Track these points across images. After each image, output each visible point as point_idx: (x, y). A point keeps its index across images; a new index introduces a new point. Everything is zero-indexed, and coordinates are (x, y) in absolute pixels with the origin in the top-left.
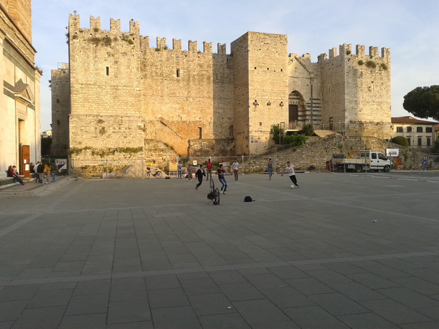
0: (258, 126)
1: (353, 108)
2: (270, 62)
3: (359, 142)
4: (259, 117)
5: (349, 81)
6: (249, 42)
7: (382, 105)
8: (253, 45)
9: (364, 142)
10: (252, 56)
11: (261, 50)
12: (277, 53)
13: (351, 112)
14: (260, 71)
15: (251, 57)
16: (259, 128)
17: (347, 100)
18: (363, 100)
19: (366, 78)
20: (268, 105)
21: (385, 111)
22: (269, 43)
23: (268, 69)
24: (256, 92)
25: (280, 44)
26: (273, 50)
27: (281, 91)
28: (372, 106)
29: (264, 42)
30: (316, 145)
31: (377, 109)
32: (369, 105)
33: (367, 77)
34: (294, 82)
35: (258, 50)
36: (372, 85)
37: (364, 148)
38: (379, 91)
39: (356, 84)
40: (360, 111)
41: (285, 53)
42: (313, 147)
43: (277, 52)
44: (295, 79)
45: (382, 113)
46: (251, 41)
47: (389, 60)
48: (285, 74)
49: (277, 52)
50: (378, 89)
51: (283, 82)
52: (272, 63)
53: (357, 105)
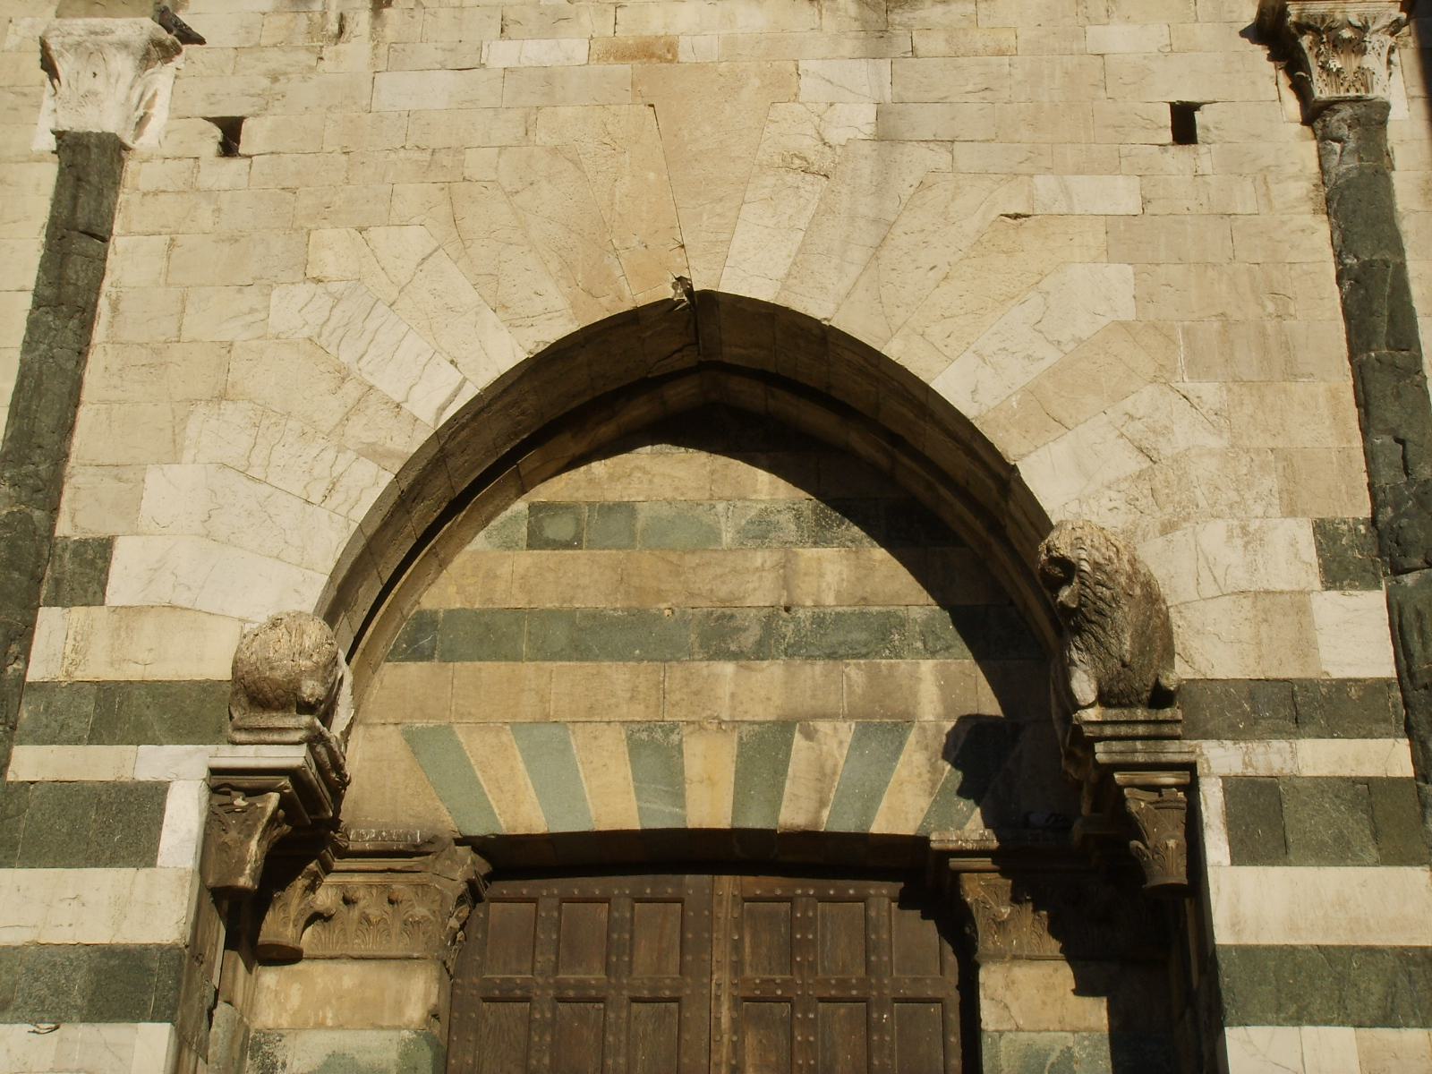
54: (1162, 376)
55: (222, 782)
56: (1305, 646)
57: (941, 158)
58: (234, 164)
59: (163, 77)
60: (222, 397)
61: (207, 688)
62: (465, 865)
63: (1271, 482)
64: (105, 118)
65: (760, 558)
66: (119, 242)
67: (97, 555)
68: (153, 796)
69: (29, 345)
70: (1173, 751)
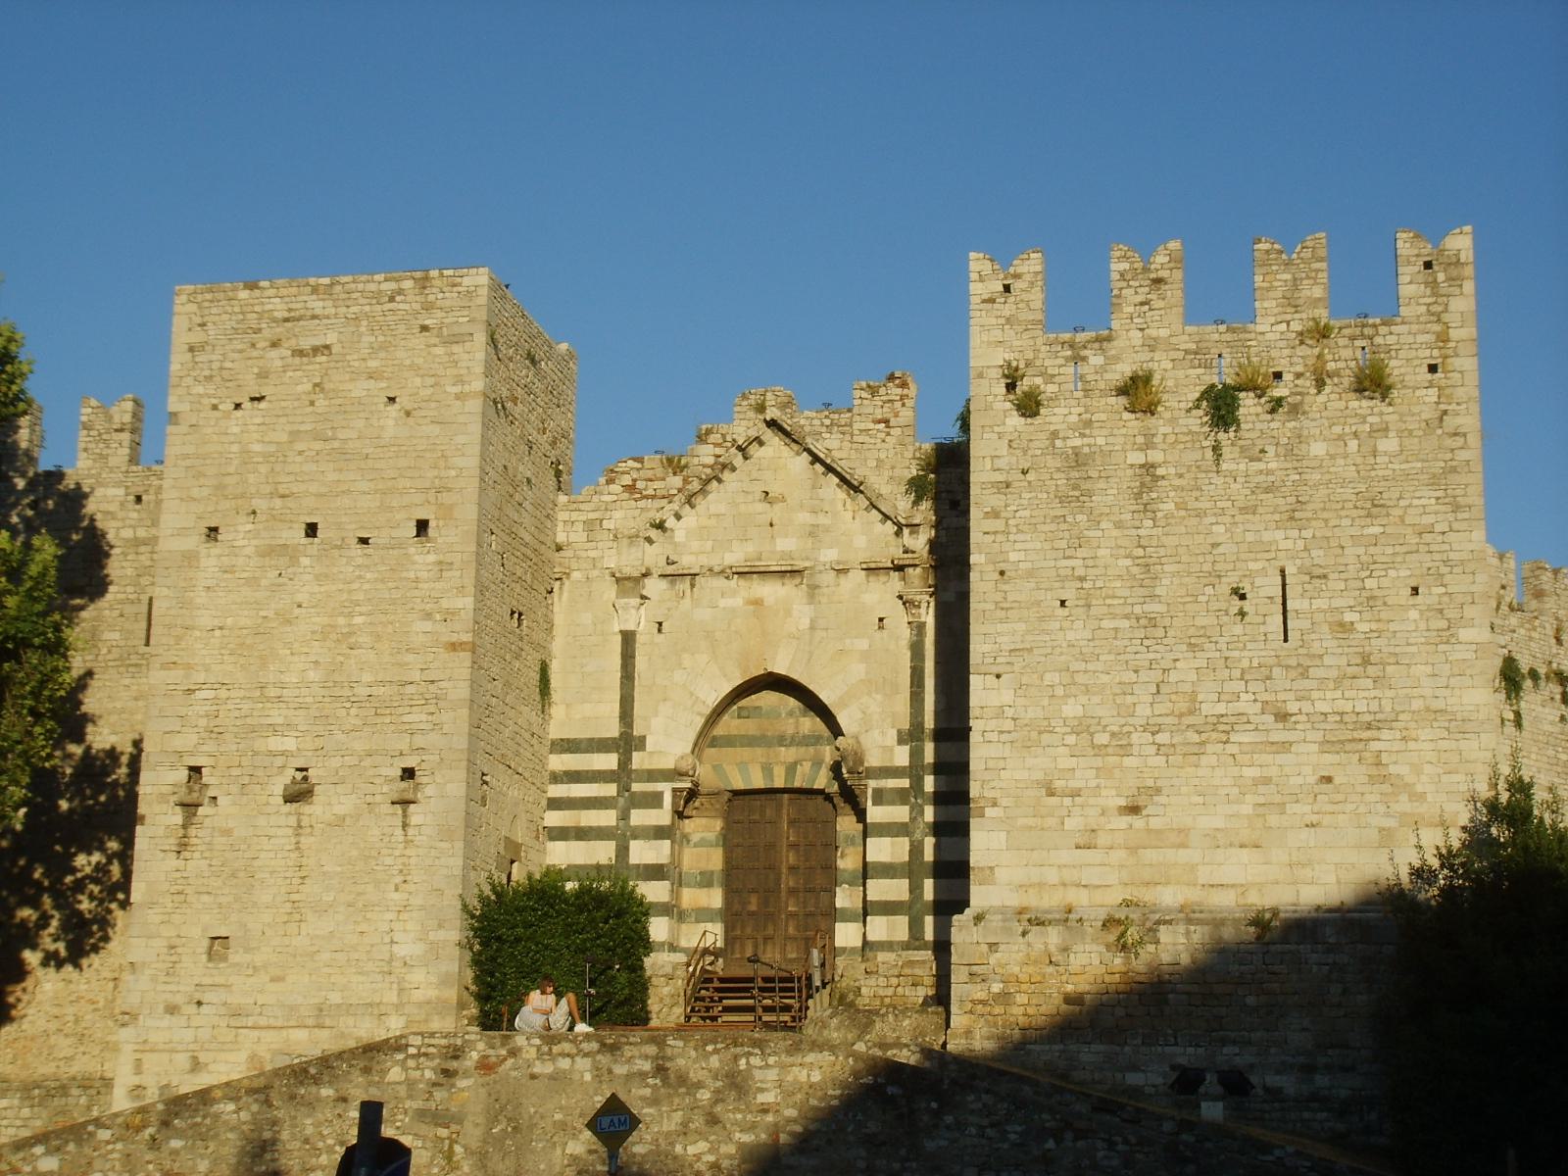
0: (194, 966)
1: (1059, 784)
2: (333, 476)
3: (647, 1092)
4: (205, 898)
5: (1013, 557)
6: (178, 361)
7: (1386, 741)
8: (209, 378)
9: (699, 1085)
10: (190, 450)
11: (263, 405)
12: (393, 409)
13: (1031, 822)
14: (249, 551)
15: (186, 456)
16: (207, 981)
17: (992, 724)
18: (1159, 709)
19: (1200, 514)
20: (291, 798)
21: (1422, 796)
22: (327, 347)
23: (312, 530)
24: (202, 709)
25: (419, 341)
26: (359, 389)
27: (410, 689)
28: (1267, 758)
29: (293, 342)
30: (217, 1116)
31: (1328, 780)
32: (1232, 749)
33: (1205, 505)
34: (757, 603)
35: (238, 406)
36: (1264, 572)
37: (691, 1150)
38: (1349, 617)
39: (1082, 579)
40: (1134, 810)
41: (458, 397)
42: (180, 1134)
43: (392, 400)
44: (770, 591)
45: (1391, 823)
46: (191, 349)
47: (1453, 334)
48: (448, 558)
49: (392, 400)
50: (1337, 603)
51: (428, 616)
52: (345, 487)
53: (1098, 762)
54: (869, 694)
55: (674, 790)
56: (891, 759)
57: (824, 634)
58: (662, 636)
59: (643, 609)
60: (665, 700)
61: (669, 770)
62: (727, 796)
63: (889, 720)
64: (630, 627)
65: (791, 721)
66: (637, 658)
67: (643, 739)
68: (662, 793)
69: (621, 689)
70: (863, 782)
